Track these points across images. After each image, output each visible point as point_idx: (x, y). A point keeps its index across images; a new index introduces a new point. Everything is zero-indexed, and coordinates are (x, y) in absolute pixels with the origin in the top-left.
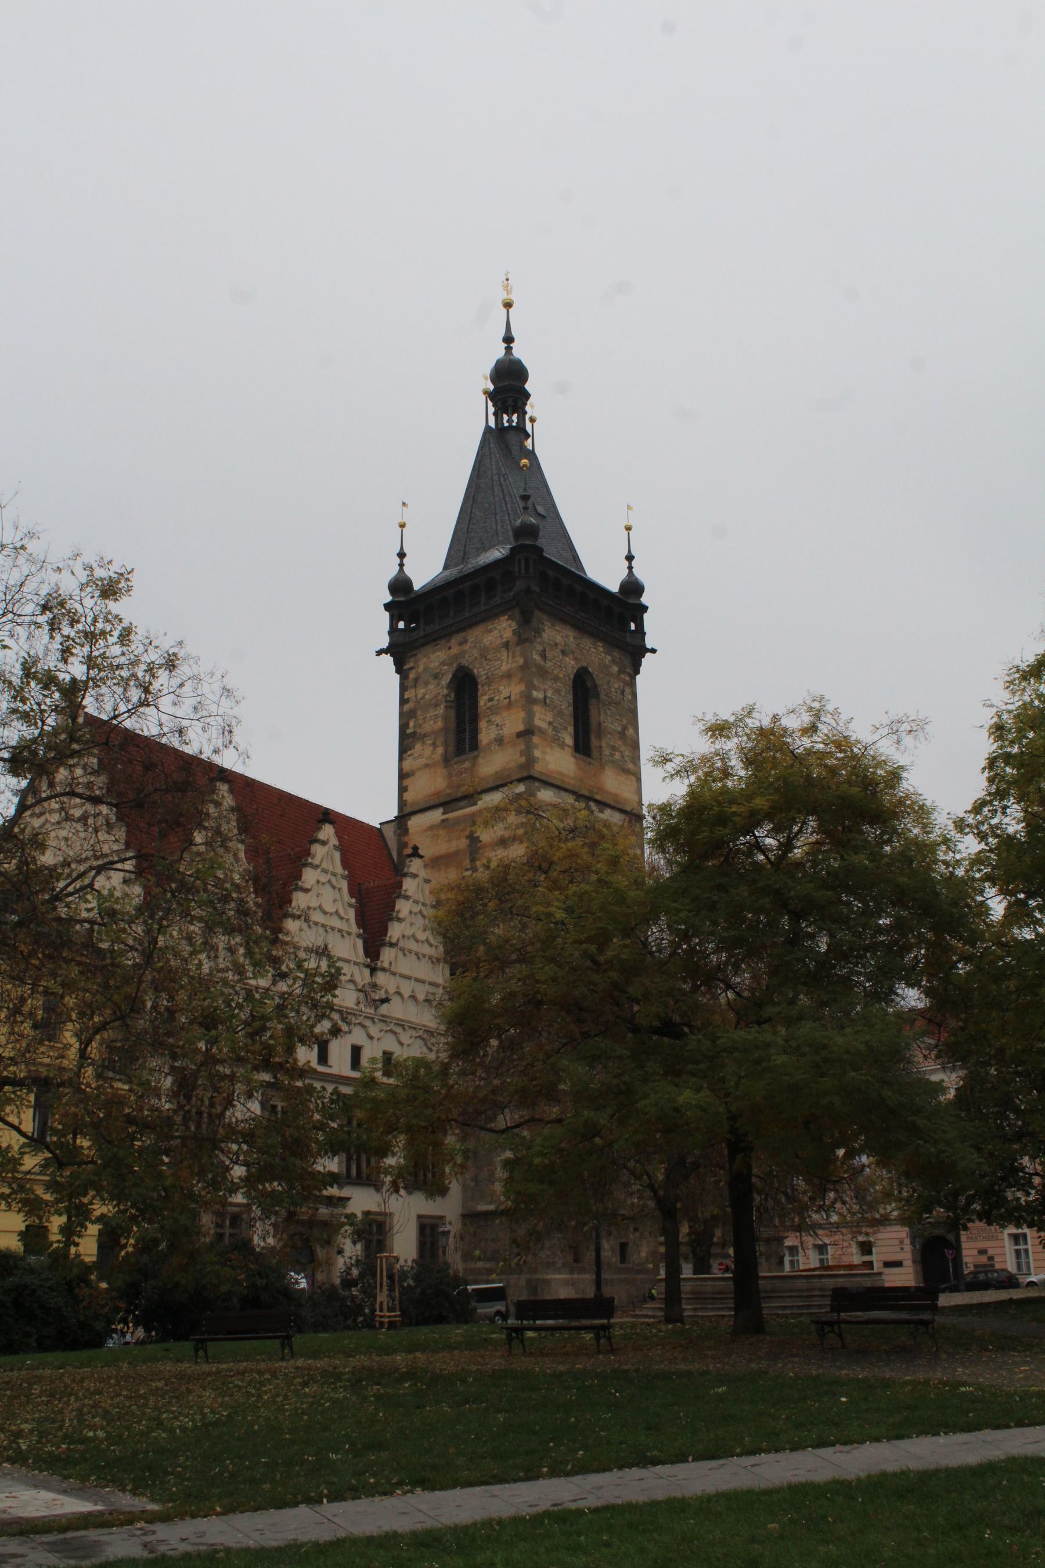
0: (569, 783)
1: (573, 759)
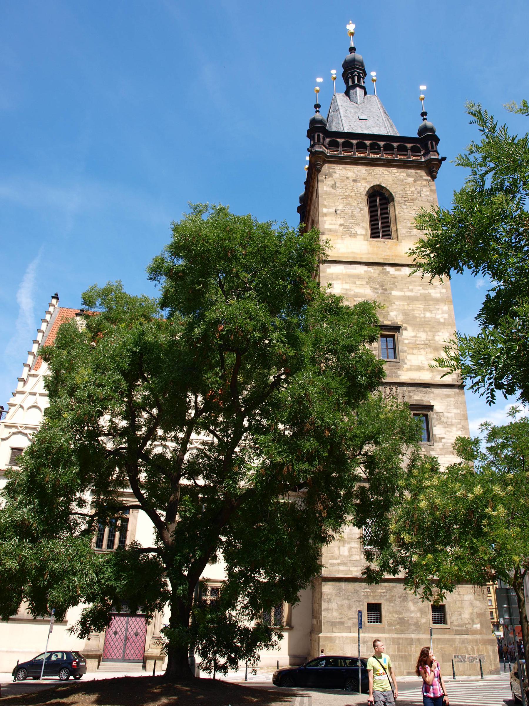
0: (361, 258)
1: (366, 243)
